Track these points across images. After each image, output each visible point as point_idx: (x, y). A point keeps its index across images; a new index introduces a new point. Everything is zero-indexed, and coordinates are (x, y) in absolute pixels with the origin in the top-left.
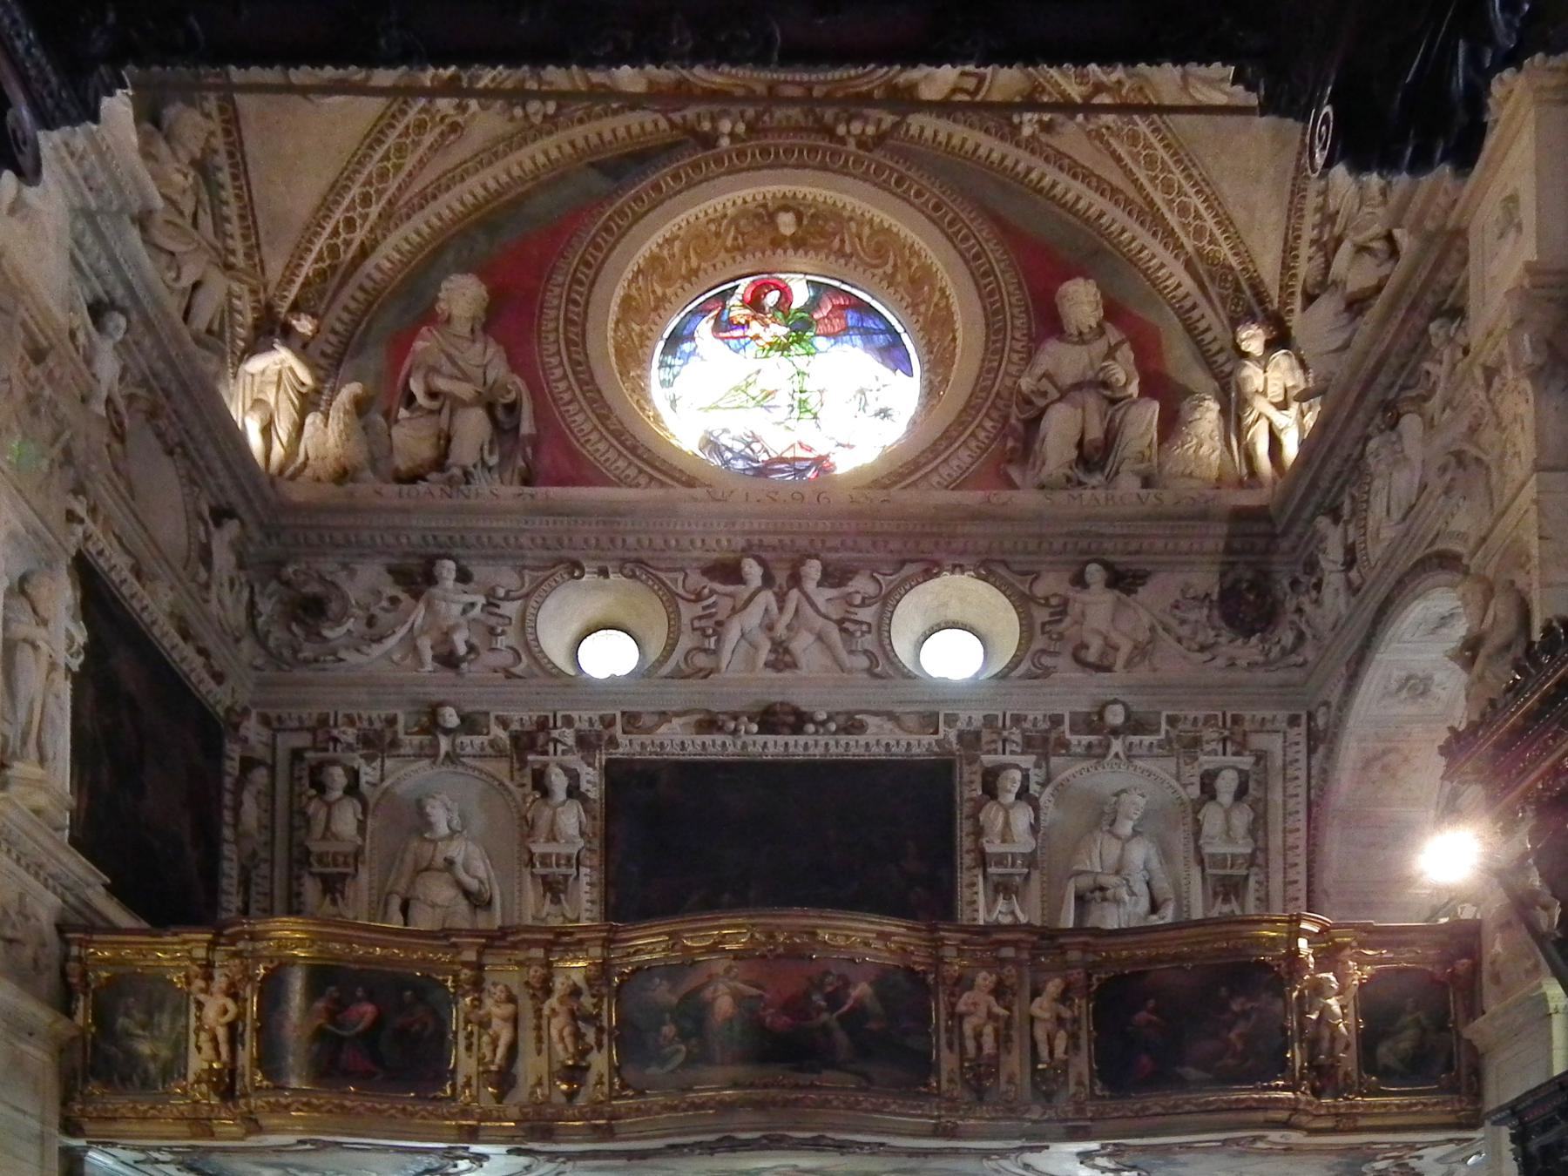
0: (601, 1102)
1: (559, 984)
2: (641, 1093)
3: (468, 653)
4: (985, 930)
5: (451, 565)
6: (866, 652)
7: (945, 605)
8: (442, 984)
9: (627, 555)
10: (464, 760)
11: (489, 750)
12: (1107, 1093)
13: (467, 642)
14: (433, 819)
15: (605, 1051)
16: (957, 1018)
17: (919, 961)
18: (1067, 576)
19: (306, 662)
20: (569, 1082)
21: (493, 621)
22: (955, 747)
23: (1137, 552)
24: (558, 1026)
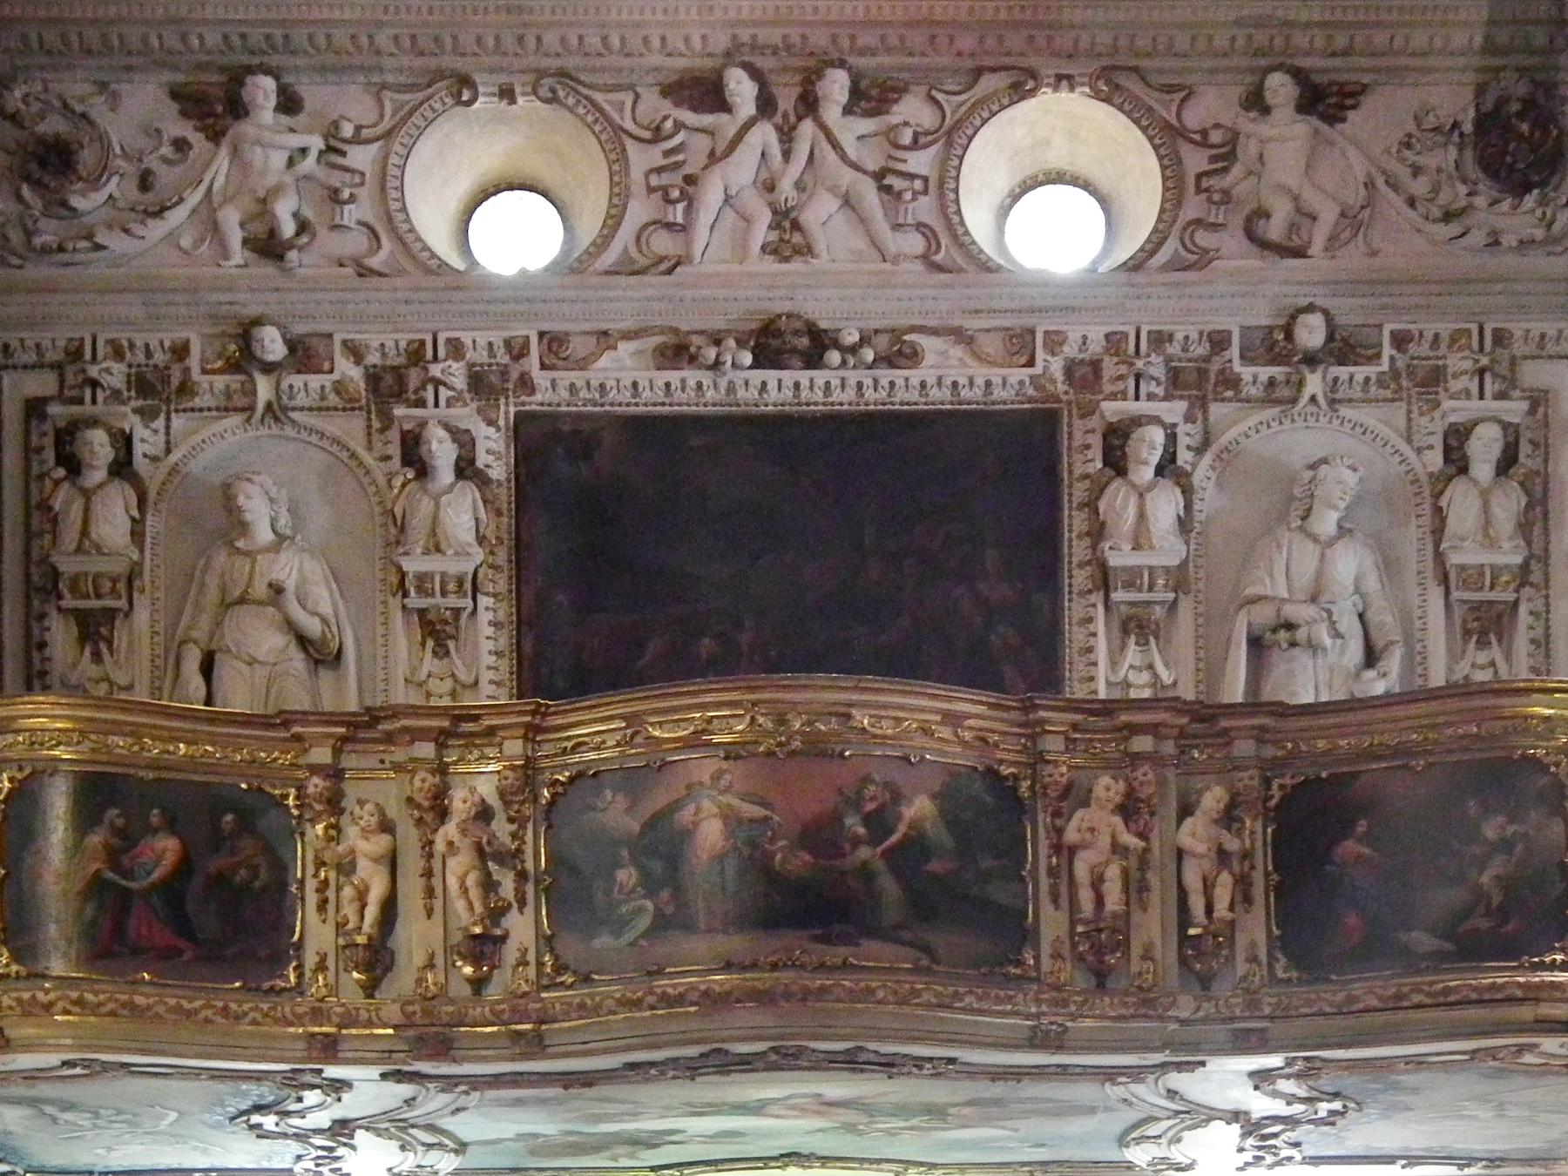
0: (525, 994)
1: (460, 802)
2: (587, 980)
3: (298, 234)
4: (1107, 709)
5: (268, 83)
6: (920, 226)
7: (1046, 143)
8: (280, 803)
9: (545, 63)
10: (295, 415)
11: (333, 399)
12: (1295, 974)
13: (295, 215)
14: (248, 517)
15: (529, 909)
16: (1065, 852)
17: (1008, 761)
18: (1236, 92)
19: (45, 250)
20: (476, 961)
21: (336, 179)
22: (1061, 387)
23: (1346, 52)
24: (458, 869)
